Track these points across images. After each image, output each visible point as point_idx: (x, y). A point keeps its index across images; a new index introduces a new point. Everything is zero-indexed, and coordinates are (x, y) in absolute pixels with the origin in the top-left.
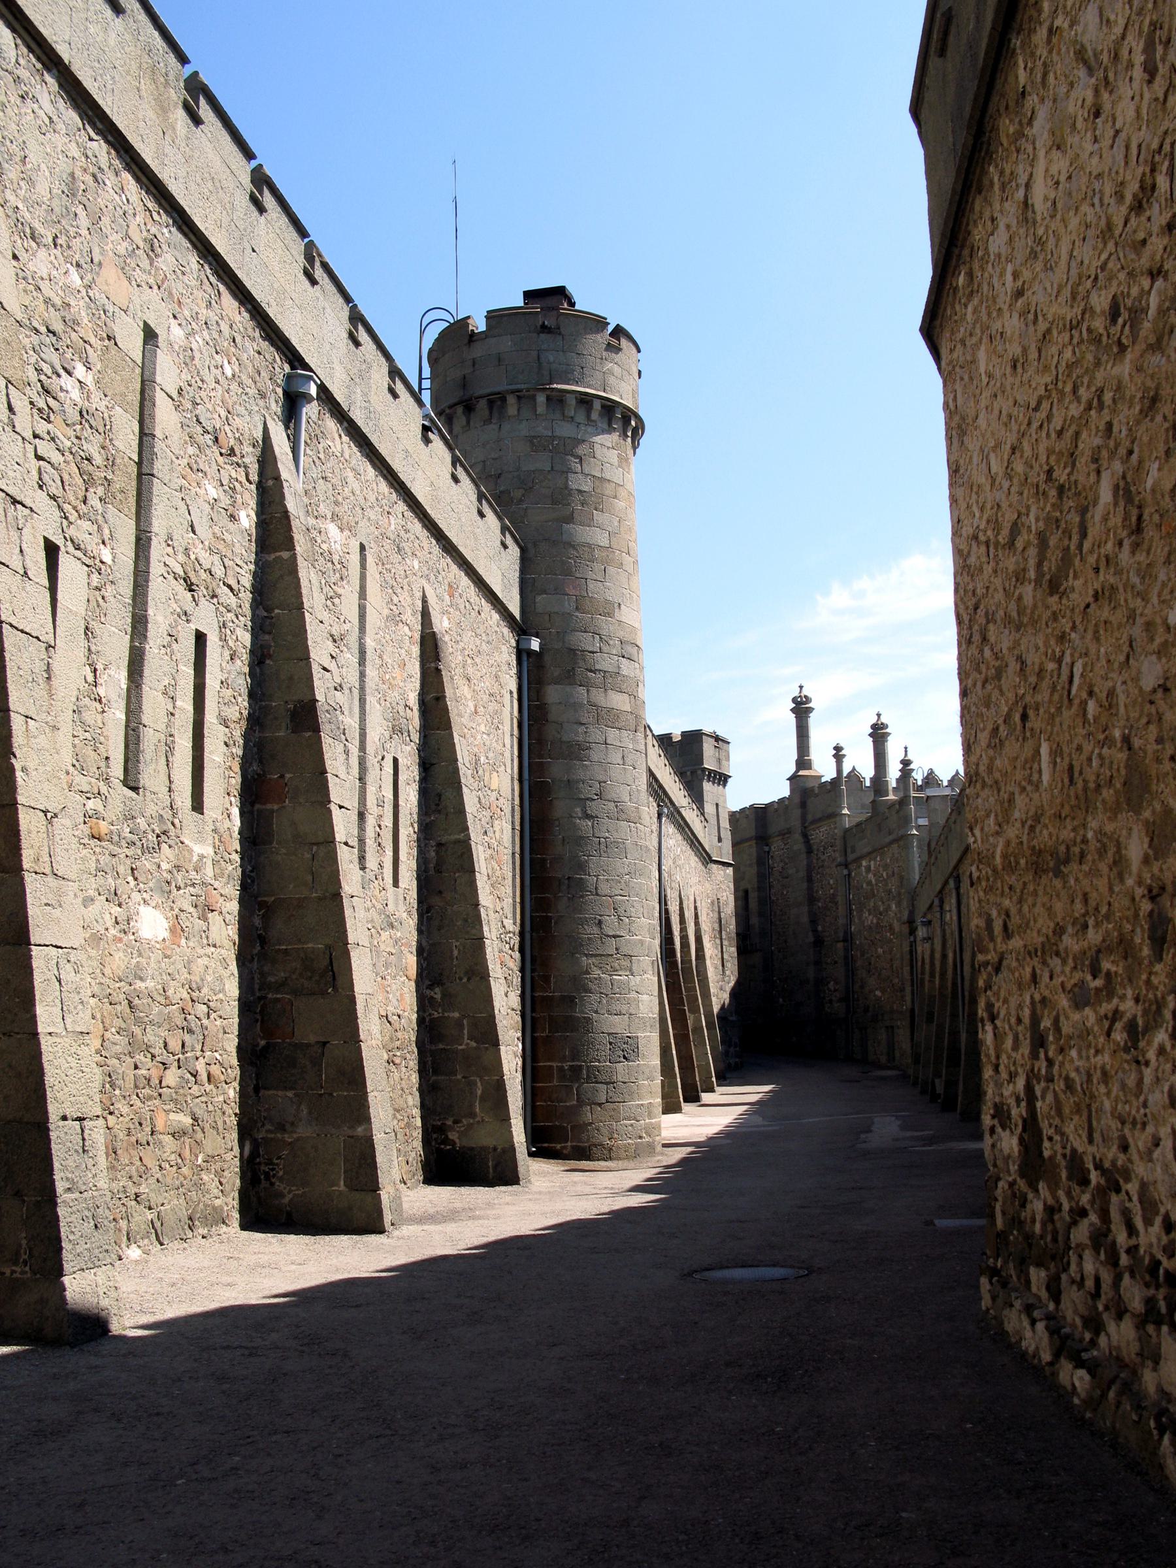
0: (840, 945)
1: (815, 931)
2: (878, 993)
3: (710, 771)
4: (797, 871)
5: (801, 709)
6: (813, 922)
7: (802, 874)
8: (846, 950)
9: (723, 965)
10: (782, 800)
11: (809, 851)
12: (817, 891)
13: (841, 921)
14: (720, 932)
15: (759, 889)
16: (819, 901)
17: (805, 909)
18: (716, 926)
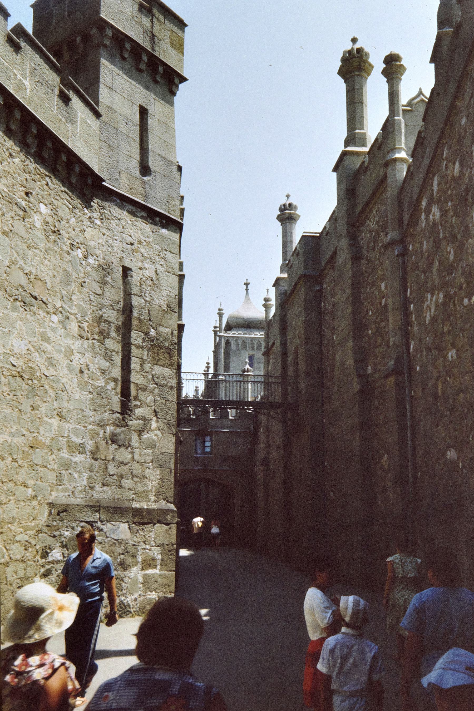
0: (391, 381)
1: (362, 376)
2: (451, 454)
3: (120, 39)
4: (343, 292)
5: (353, 66)
6: (361, 362)
7: (348, 291)
8: (400, 387)
9: (125, 393)
10: (333, 218)
11: (356, 258)
12: (368, 312)
13: (393, 339)
14: (126, 329)
15: (307, 341)
16: (368, 328)
17: (350, 344)
18: (113, 316)
